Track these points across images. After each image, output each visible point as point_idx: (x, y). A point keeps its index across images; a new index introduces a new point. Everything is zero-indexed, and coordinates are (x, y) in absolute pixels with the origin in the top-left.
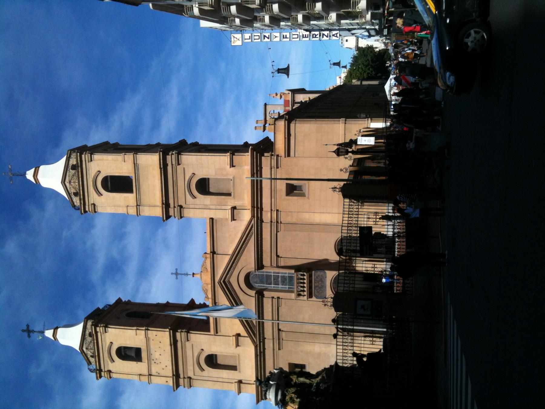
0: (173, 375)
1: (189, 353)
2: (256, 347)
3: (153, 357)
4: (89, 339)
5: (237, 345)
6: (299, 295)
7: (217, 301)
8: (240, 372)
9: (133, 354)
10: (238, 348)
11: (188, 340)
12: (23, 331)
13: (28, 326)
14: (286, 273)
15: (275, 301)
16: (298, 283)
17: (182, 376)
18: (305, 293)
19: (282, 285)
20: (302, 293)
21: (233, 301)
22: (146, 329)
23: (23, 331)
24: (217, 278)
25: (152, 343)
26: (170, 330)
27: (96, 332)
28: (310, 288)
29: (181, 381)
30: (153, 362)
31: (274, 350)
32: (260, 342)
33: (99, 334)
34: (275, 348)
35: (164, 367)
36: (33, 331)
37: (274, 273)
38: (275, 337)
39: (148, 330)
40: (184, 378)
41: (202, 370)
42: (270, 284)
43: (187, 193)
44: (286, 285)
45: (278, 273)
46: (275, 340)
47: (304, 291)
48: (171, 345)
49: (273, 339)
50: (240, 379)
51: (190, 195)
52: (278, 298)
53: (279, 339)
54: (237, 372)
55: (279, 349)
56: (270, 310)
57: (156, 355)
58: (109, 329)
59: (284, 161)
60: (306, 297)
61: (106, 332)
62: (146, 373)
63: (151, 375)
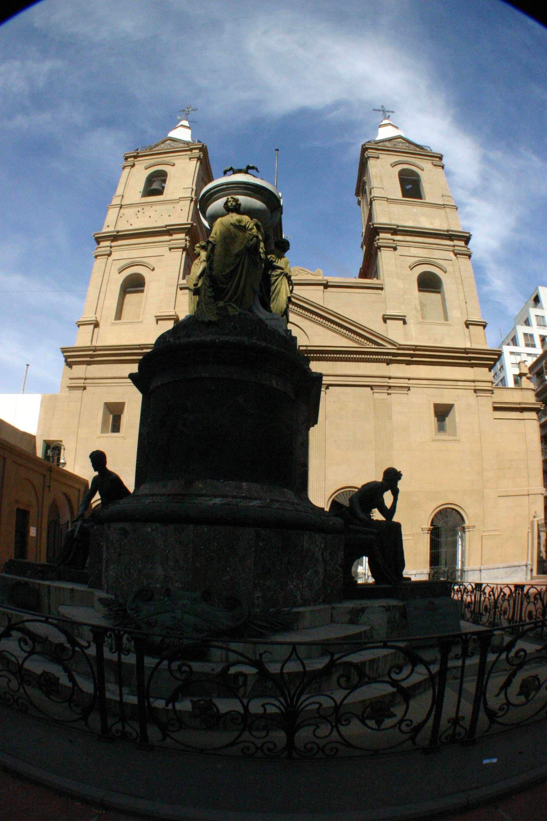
0: (118, 232)
1: (149, 252)
3: (146, 208)
8: (113, 324)
9: (155, 186)
11: (170, 249)
17: (113, 244)
22: (192, 198)
25: (171, 206)
26: (192, 225)
27: (191, 150)
30: (140, 209)
35: (130, 222)
39: (191, 201)
40: (111, 247)
41: (121, 271)
43: (417, 259)
48: (166, 226)
50: (101, 325)
51: (415, 262)
54: (113, 321)
57: (149, 211)
58: (195, 162)
59: (487, 402)
61: (190, 159)
63: (121, 208)
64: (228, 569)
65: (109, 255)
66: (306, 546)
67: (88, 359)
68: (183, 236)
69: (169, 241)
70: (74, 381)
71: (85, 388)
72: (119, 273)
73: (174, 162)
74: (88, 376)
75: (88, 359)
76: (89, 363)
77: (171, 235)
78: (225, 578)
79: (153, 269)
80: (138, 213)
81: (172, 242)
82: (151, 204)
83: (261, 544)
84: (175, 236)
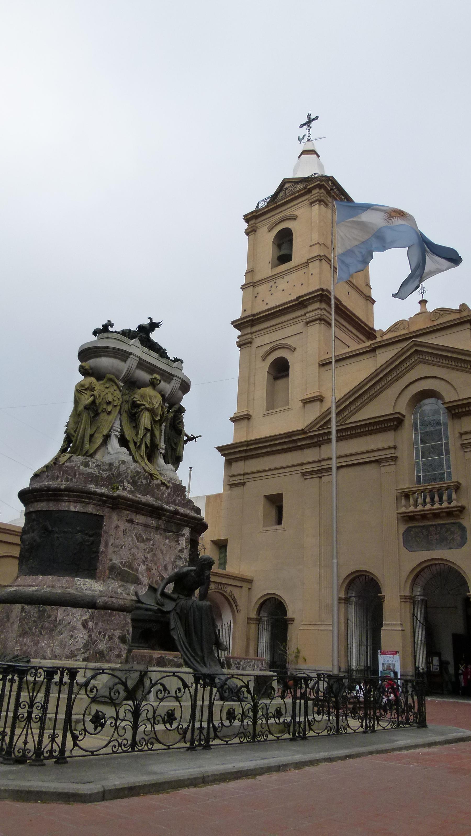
0: (254, 315)
2: (303, 432)
4: (300, 186)
5: (306, 402)
6: (407, 496)
7: (378, 352)
10: (301, 404)
11: (307, 323)
12: (309, 116)
13: (316, 118)
14: (449, 467)
15: (390, 453)
16: (431, 491)
17: (254, 329)
18: (412, 509)
19: (424, 465)
20: (411, 501)
21: (381, 376)
23: (309, 116)
24: (421, 339)
25: (301, 272)
28: (424, 517)
29: (248, 330)
30: (272, 283)
31: (301, 465)
32: (312, 437)
33: (307, 197)
34: (305, 467)
36: (309, 127)
37: (447, 444)
38: (323, 463)
42: (422, 441)
44: (424, 471)
45: (447, 453)
46: (318, 464)
47: (416, 505)
49: (319, 461)
50: (254, 416)
52: (395, 458)
53: (320, 471)
55: (304, 474)
56: (372, 447)
57: (282, 284)
60: (403, 510)
62: (258, 277)
64: (4, 631)
65: (251, 343)
66: (60, 617)
67: (244, 455)
68: (317, 305)
69: (305, 315)
70: (234, 478)
71: (244, 483)
72: (264, 360)
73: (294, 213)
74: (246, 471)
75: (244, 455)
76: (245, 458)
77: (306, 307)
78: (2, 637)
79: (295, 349)
80: (272, 289)
81: (307, 315)
82: (289, 272)
83: (24, 615)
84: (310, 308)
